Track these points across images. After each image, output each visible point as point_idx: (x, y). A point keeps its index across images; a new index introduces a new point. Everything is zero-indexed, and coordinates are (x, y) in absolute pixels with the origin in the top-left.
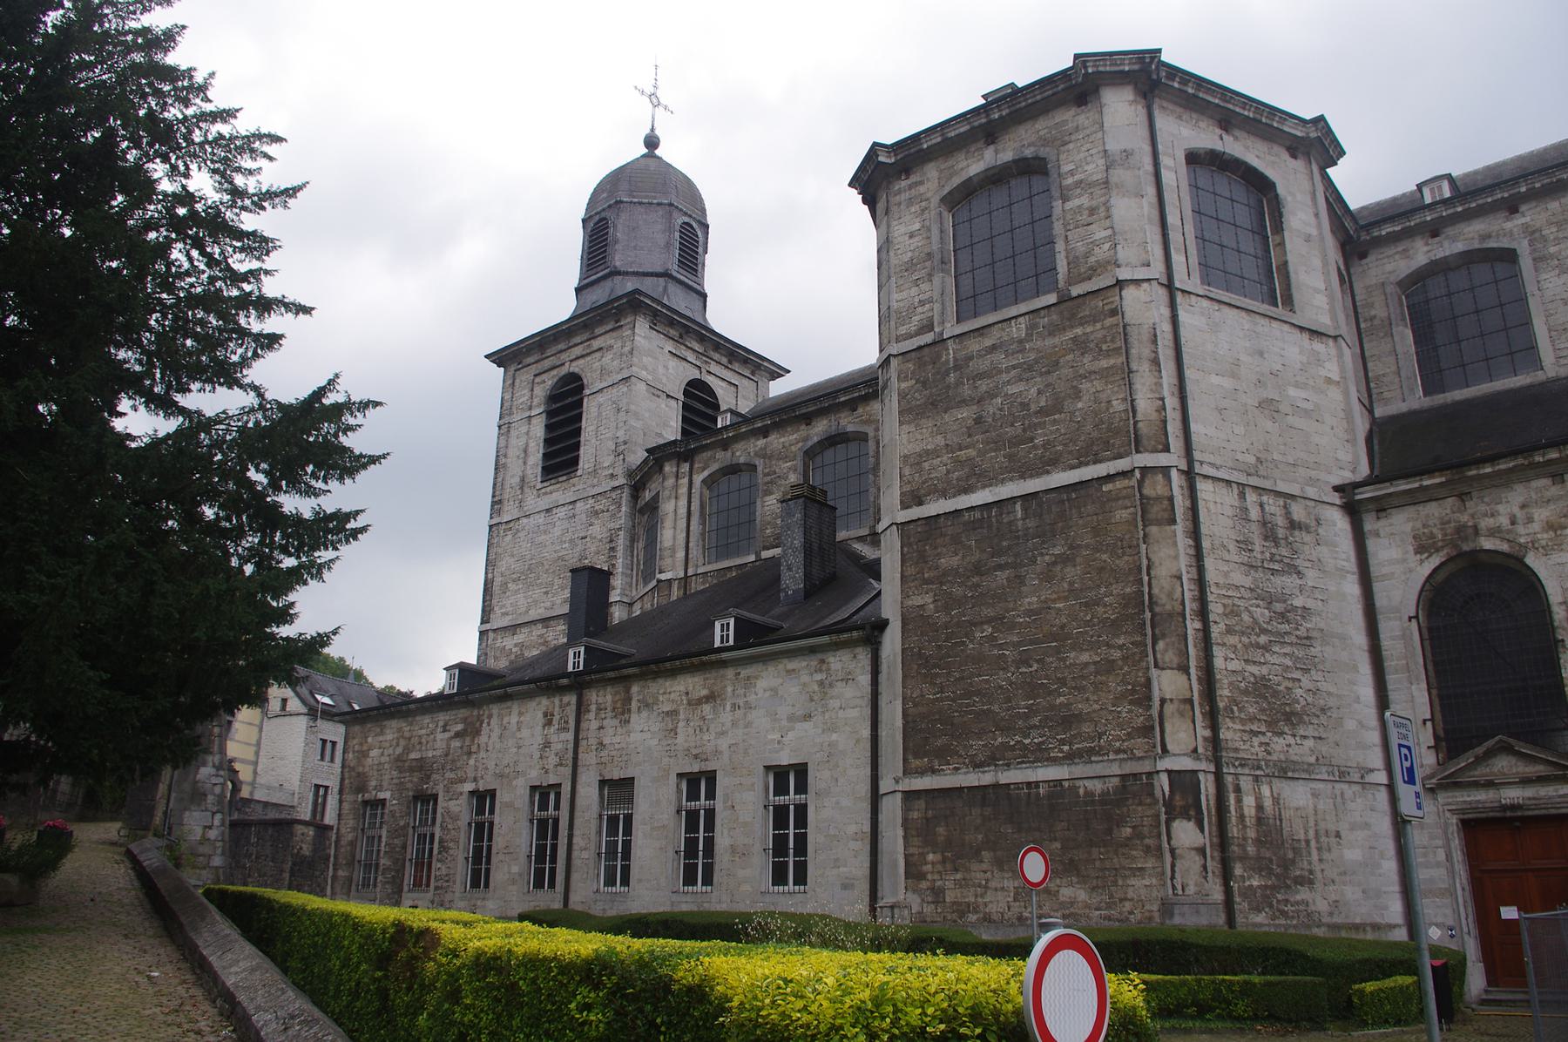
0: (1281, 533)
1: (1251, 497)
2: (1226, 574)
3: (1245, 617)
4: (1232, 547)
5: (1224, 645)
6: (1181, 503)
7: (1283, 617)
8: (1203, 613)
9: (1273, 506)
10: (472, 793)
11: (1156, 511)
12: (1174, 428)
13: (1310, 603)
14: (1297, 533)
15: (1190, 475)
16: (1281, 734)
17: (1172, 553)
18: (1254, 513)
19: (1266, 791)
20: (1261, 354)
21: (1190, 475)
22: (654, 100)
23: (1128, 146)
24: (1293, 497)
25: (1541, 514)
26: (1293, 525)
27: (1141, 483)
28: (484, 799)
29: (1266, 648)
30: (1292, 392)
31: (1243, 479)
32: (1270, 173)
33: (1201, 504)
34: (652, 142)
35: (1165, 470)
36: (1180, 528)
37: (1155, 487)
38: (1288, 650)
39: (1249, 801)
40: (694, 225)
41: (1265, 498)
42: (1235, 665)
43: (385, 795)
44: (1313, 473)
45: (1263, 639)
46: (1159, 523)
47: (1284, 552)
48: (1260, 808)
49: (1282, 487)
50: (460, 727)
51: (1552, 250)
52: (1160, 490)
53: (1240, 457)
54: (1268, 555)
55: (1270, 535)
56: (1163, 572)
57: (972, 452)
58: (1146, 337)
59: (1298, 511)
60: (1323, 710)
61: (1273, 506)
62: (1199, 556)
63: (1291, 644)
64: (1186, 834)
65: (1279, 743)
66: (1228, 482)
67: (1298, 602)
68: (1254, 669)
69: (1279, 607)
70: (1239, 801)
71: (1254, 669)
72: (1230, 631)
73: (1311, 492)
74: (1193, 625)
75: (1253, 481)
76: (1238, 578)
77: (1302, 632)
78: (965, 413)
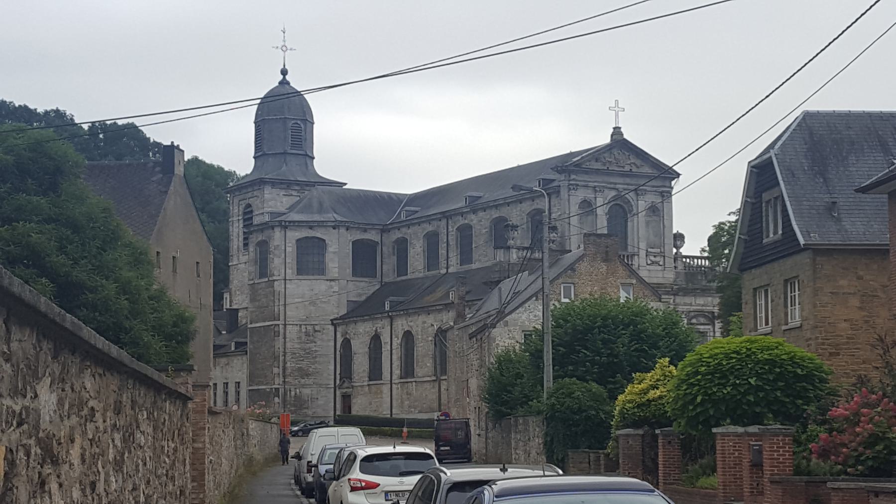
0: (311, 334)
1: (303, 327)
2: (293, 346)
4: (296, 339)
6: (282, 331)
7: (308, 353)
8: (285, 356)
9: (309, 328)
11: (276, 334)
12: (282, 318)
13: (317, 349)
15: (285, 325)
21: (285, 325)
24: (316, 325)
26: (316, 331)
29: (303, 360)
31: (301, 323)
33: (288, 332)
35: (279, 325)
36: (281, 337)
37: (276, 329)
41: (308, 326)
44: (324, 317)
55: (307, 334)
56: (277, 347)
59: (317, 328)
61: (309, 328)
62: (285, 343)
66: (297, 325)
69: (307, 351)
72: (292, 358)
73: (323, 322)
74: (281, 358)
75: (304, 323)
76: (297, 346)
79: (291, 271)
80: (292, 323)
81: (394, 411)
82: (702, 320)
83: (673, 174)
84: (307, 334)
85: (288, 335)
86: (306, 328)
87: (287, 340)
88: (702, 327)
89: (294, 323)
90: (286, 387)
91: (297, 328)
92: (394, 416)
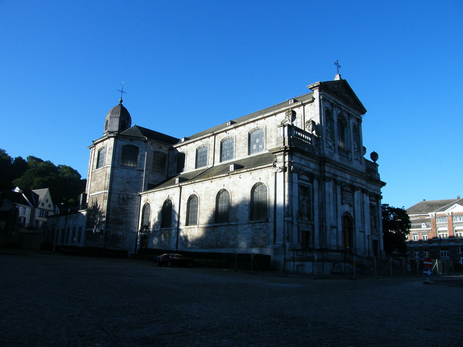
0: (126, 199)
1: (121, 195)
3: (116, 211)
5: (112, 214)
7: (123, 211)
9: (125, 196)
10: (57, 229)
13: (128, 209)
14: (129, 199)
16: (119, 225)
17: (106, 203)
18: (121, 197)
19: (115, 232)
20: (129, 175)
22: (122, 92)
23: (111, 147)
24: (129, 195)
25: (152, 198)
26: (128, 198)
27: (104, 194)
28: (58, 229)
29: (119, 215)
30: (133, 180)
31: (120, 193)
32: (138, 146)
34: (121, 101)
38: (123, 215)
39: (112, 233)
40: (125, 120)
41: (124, 195)
42: (113, 217)
43: (50, 229)
45: (119, 214)
46: (105, 199)
47: (126, 202)
48: (113, 234)
49: (127, 193)
50: (57, 220)
51: (189, 153)
52: (106, 195)
53: (121, 190)
54: (122, 203)
57: (95, 187)
58: (108, 175)
59: (129, 196)
60: (127, 222)
63: (124, 214)
64: (101, 237)
65: (118, 226)
66: (118, 194)
67: (126, 209)
68: (116, 217)
69: (122, 209)
70: (110, 233)
71: (116, 217)
72: (113, 213)
75: (123, 193)
77: (126, 212)
78: (95, 182)
79: (117, 162)
80: (115, 192)
81: (179, 246)
82: (374, 199)
83: (363, 109)
84: (123, 199)
85: (112, 197)
86: (123, 196)
87: (111, 202)
88: (373, 203)
89: (116, 192)
90: (108, 229)
91: (117, 196)
92: (178, 250)
